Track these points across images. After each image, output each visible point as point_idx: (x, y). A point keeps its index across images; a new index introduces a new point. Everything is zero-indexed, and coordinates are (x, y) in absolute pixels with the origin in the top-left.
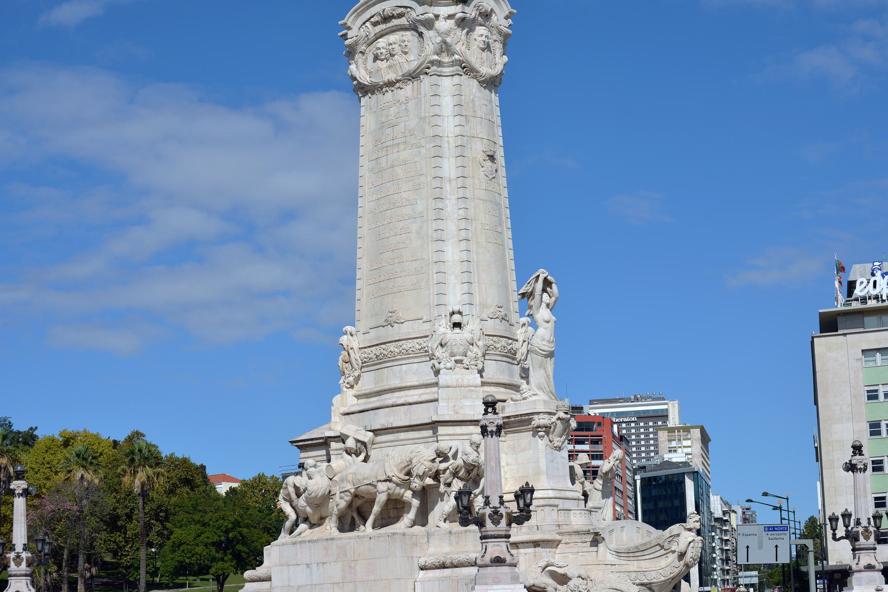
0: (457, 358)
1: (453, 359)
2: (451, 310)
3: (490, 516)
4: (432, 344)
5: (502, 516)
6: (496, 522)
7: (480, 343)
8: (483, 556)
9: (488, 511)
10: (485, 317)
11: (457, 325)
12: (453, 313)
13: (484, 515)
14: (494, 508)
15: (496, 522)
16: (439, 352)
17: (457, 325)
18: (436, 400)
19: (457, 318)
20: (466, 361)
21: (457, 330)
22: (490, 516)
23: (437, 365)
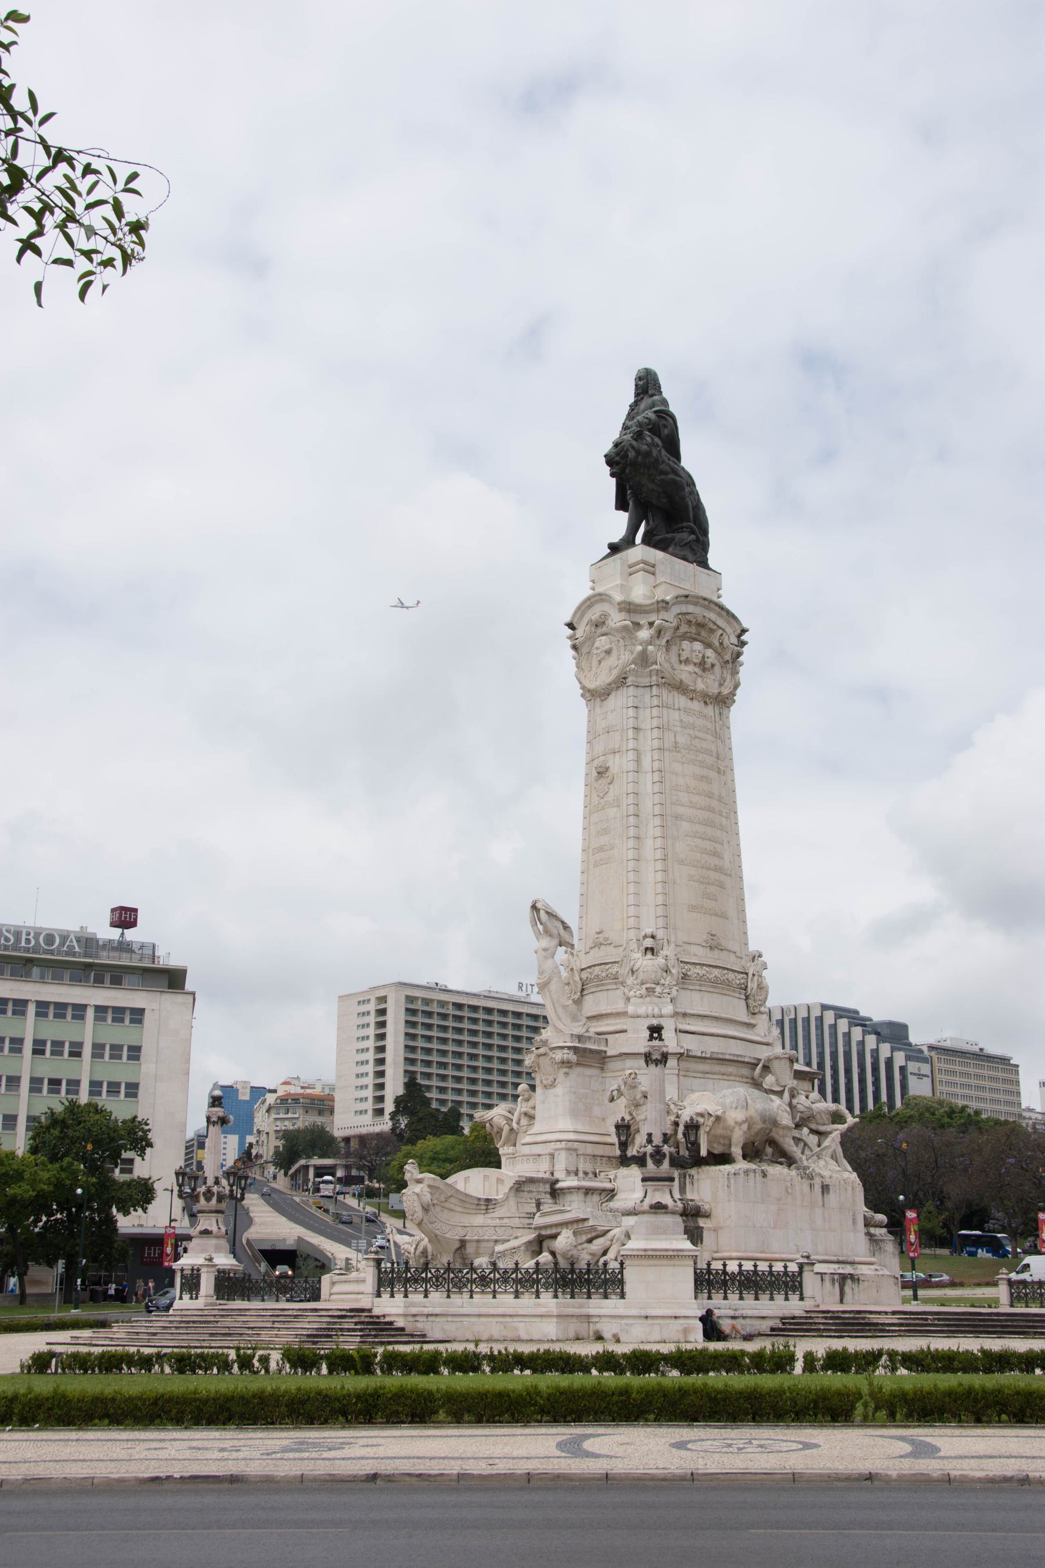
0: (648, 985)
1: (644, 987)
2: (643, 934)
3: (652, 1156)
4: (624, 971)
5: (664, 1155)
6: (658, 1162)
7: (674, 971)
8: (642, 1201)
9: (649, 1149)
10: (680, 943)
11: (651, 950)
12: (645, 937)
13: (645, 1154)
14: (657, 1146)
15: (658, 1162)
16: (630, 980)
17: (651, 950)
18: (625, 1031)
19: (649, 943)
20: (658, 989)
21: (649, 956)
22: (652, 1156)
23: (626, 991)
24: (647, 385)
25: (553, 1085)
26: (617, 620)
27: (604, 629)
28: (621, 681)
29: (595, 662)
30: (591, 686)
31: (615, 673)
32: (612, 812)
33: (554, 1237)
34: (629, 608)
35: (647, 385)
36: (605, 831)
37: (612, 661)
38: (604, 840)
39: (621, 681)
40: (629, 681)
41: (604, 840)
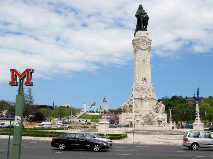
24: (141, 7)
25: (147, 102)
26: (147, 41)
27: (144, 41)
28: (146, 49)
29: (142, 45)
30: (141, 47)
31: (146, 48)
32: (146, 66)
33: (161, 121)
34: (149, 40)
35: (141, 7)
36: (145, 69)
37: (145, 46)
38: (144, 70)
39: (146, 49)
40: (148, 49)
41: (144, 70)
